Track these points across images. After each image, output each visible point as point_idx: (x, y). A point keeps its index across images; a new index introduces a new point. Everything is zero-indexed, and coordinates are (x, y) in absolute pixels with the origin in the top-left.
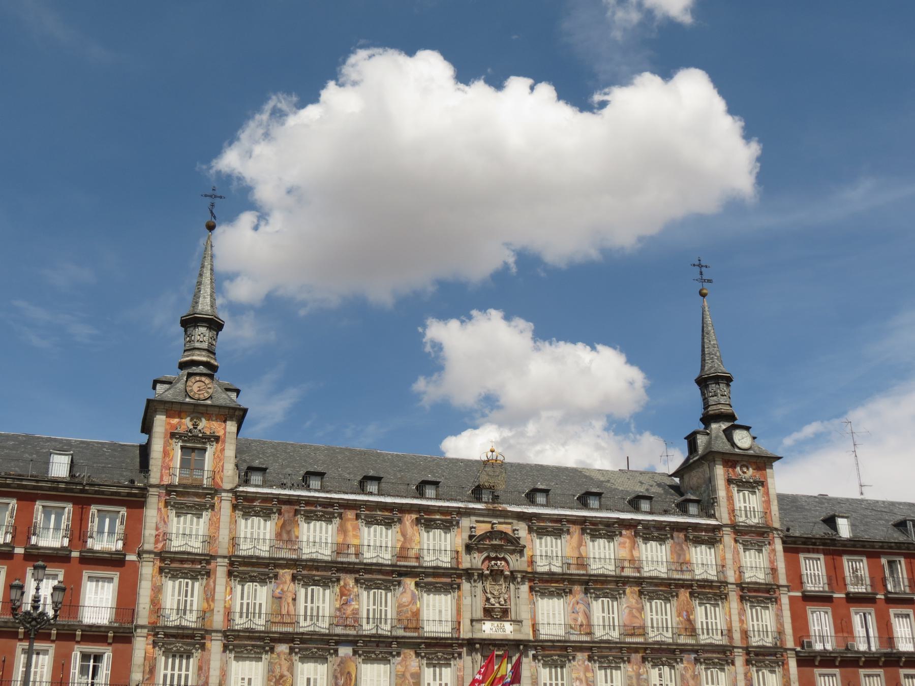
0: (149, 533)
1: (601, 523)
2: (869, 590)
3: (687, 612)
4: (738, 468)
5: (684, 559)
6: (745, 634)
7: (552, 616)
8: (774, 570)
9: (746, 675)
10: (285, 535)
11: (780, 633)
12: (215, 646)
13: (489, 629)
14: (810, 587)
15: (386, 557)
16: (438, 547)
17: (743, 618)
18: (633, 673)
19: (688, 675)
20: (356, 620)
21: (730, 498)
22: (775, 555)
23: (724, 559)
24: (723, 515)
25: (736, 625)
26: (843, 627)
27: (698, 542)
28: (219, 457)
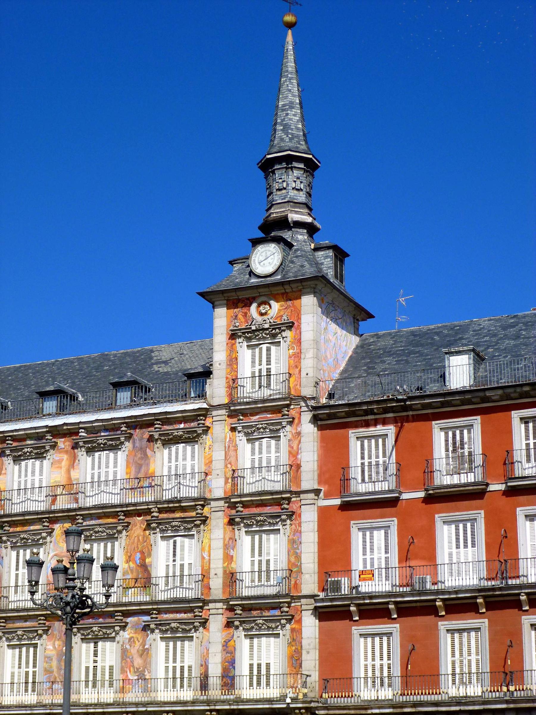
1: (29, 437)
2: (480, 478)
3: (142, 553)
5: (146, 474)
6: (231, 578)
8: (295, 467)
9: (226, 645)
11: (293, 570)
14: (362, 488)
17: (232, 553)
18: (54, 652)
19: (134, 651)
21: (233, 361)
22: (300, 442)
23: (210, 462)
24: (217, 390)
25: (217, 566)
26: (417, 548)
27: (170, 441)
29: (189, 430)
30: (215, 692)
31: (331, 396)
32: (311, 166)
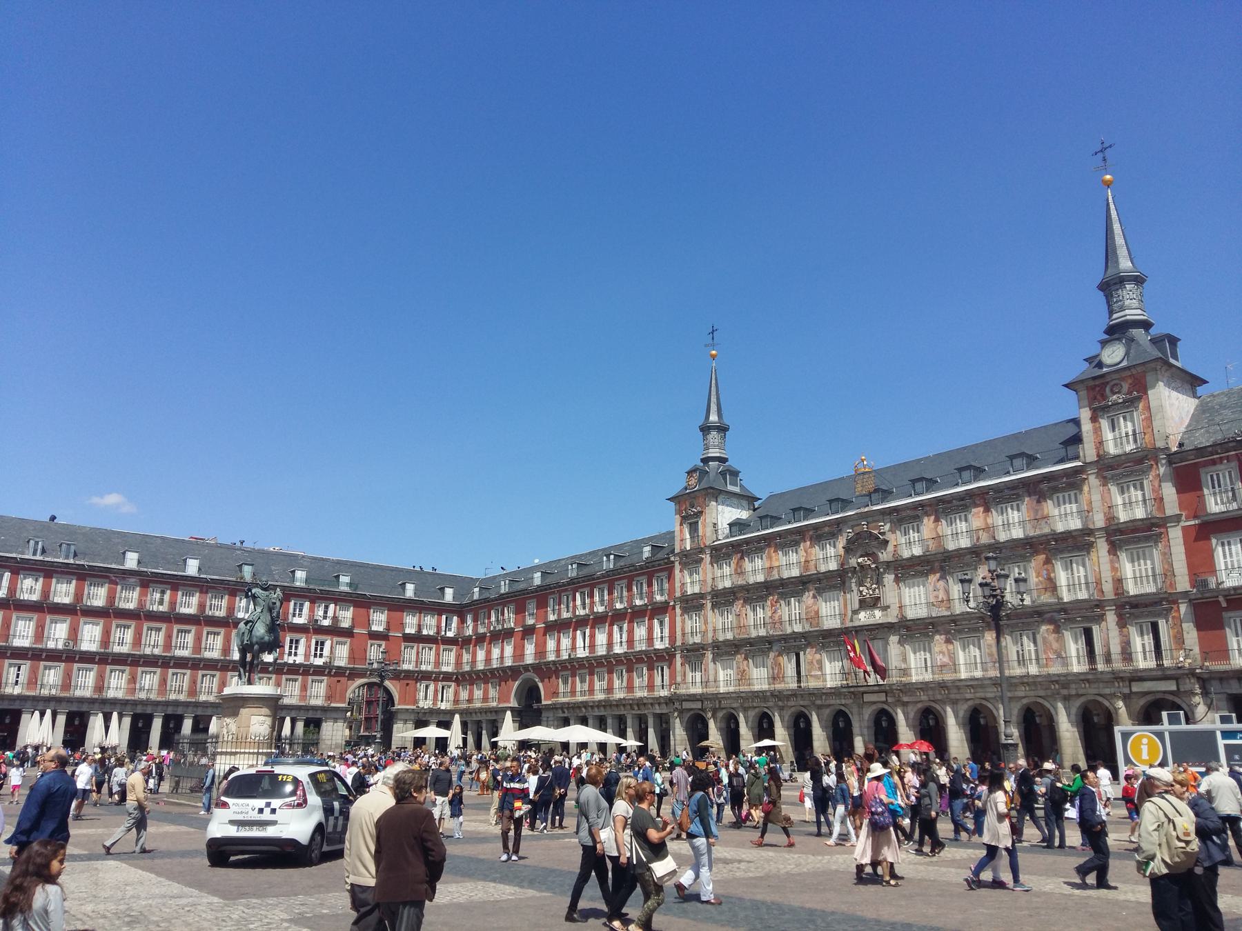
0: (678, 585)
4: (1108, 389)
6: (1119, 582)
7: (915, 599)
10: (740, 572)
11: (1169, 573)
12: (709, 655)
13: (864, 618)
15: (795, 572)
16: (828, 557)
20: (781, 623)
24: (1088, 451)
25: (1107, 575)
28: (704, 526)
29: (1070, 483)
30: (1118, 665)
31: (1181, 445)
32: (1139, 280)
